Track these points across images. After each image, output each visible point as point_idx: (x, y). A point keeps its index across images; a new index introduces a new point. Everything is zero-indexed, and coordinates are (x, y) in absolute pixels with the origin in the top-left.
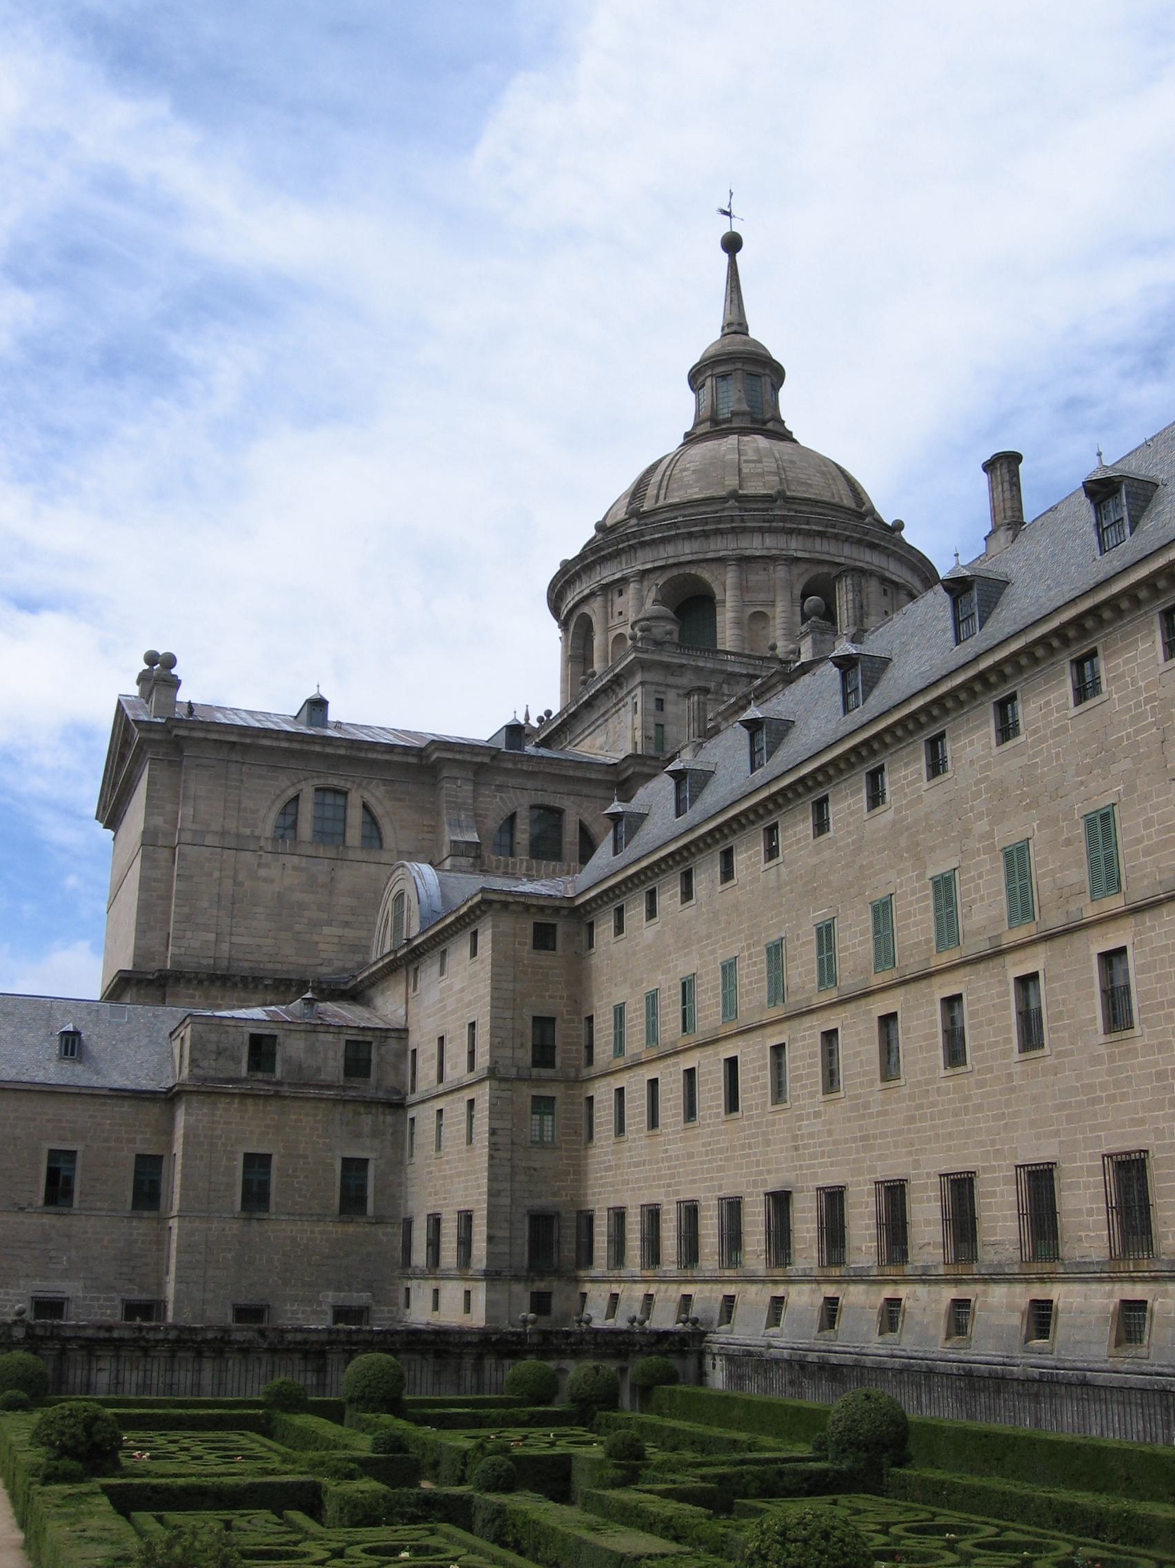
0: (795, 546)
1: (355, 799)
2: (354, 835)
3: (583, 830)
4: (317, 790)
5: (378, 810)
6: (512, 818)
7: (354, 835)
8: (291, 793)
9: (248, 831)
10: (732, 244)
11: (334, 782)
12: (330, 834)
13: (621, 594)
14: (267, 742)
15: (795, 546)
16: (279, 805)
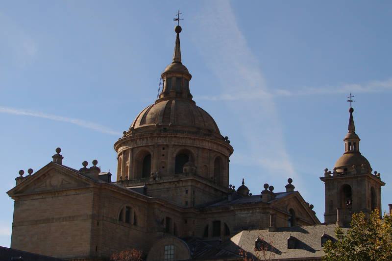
0: (215, 147)
1: (133, 211)
2: (132, 221)
3: (175, 224)
4: (127, 207)
5: (137, 214)
6: (163, 220)
7: (132, 221)
8: (122, 207)
9: (114, 218)
10: (178, 30)
11: (130, 205)
12: (128, 221)
13: (164, 149)
14: (121, 192)
15: (215, 147)
16: (120, 211)
